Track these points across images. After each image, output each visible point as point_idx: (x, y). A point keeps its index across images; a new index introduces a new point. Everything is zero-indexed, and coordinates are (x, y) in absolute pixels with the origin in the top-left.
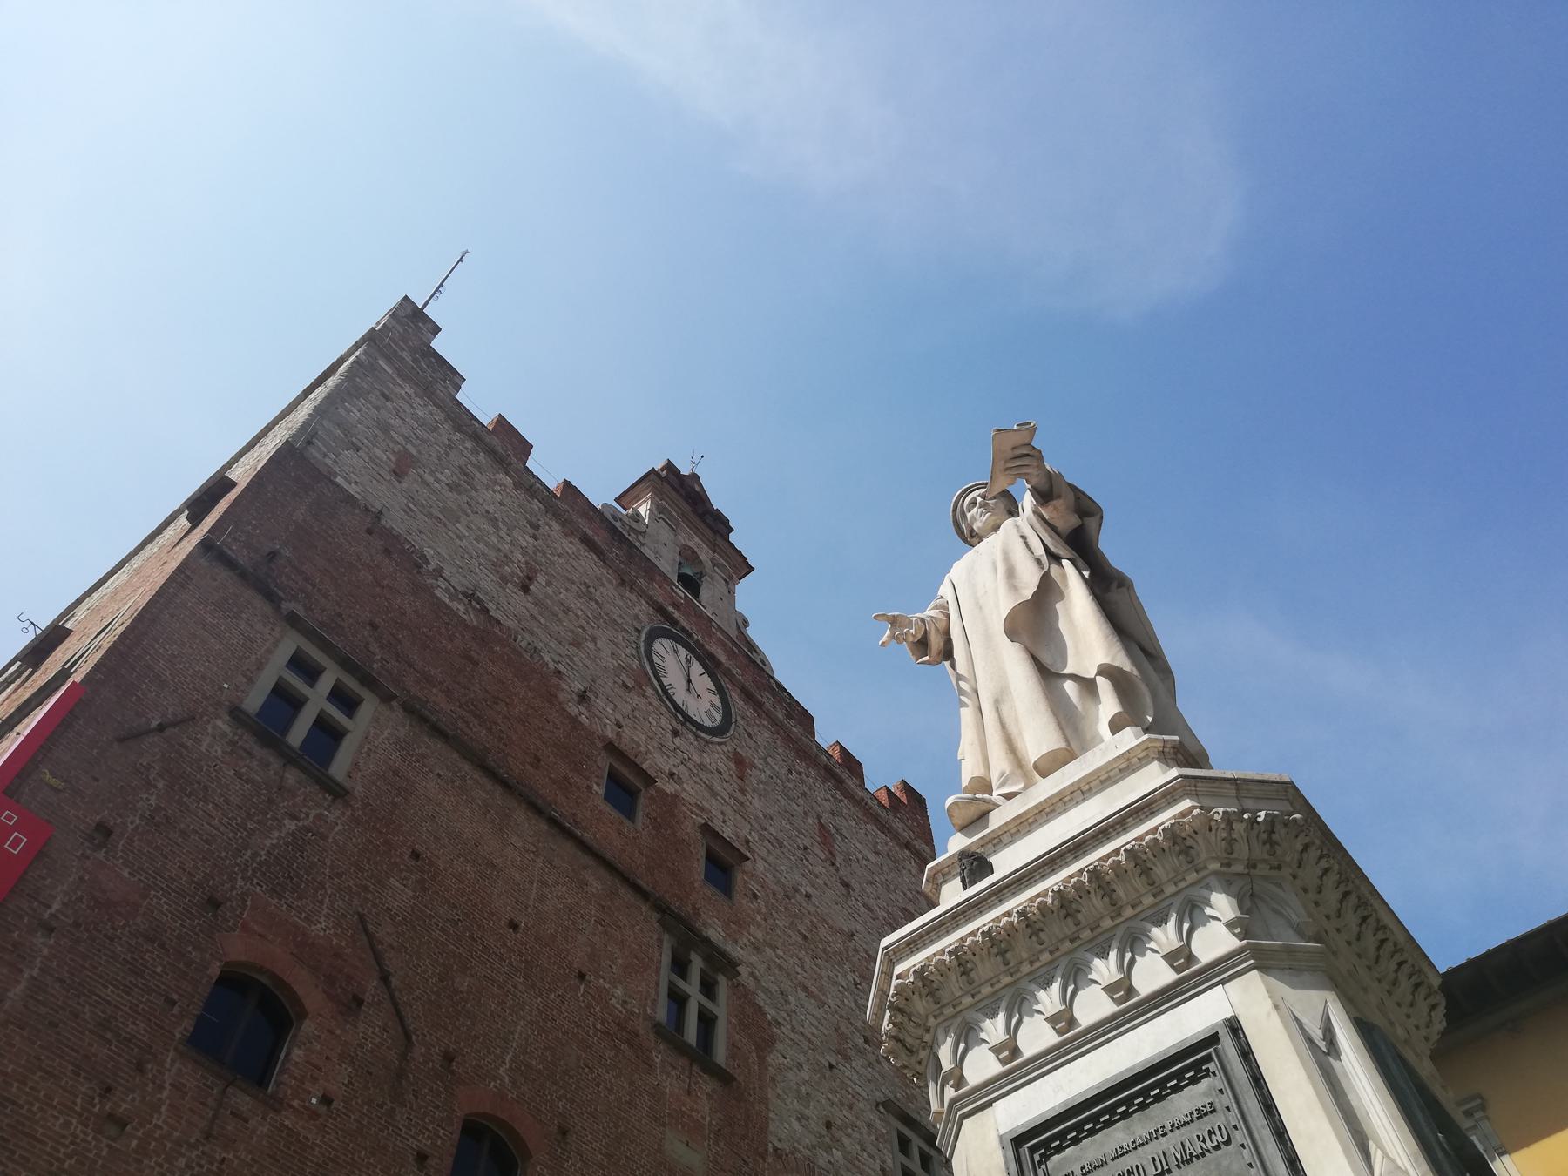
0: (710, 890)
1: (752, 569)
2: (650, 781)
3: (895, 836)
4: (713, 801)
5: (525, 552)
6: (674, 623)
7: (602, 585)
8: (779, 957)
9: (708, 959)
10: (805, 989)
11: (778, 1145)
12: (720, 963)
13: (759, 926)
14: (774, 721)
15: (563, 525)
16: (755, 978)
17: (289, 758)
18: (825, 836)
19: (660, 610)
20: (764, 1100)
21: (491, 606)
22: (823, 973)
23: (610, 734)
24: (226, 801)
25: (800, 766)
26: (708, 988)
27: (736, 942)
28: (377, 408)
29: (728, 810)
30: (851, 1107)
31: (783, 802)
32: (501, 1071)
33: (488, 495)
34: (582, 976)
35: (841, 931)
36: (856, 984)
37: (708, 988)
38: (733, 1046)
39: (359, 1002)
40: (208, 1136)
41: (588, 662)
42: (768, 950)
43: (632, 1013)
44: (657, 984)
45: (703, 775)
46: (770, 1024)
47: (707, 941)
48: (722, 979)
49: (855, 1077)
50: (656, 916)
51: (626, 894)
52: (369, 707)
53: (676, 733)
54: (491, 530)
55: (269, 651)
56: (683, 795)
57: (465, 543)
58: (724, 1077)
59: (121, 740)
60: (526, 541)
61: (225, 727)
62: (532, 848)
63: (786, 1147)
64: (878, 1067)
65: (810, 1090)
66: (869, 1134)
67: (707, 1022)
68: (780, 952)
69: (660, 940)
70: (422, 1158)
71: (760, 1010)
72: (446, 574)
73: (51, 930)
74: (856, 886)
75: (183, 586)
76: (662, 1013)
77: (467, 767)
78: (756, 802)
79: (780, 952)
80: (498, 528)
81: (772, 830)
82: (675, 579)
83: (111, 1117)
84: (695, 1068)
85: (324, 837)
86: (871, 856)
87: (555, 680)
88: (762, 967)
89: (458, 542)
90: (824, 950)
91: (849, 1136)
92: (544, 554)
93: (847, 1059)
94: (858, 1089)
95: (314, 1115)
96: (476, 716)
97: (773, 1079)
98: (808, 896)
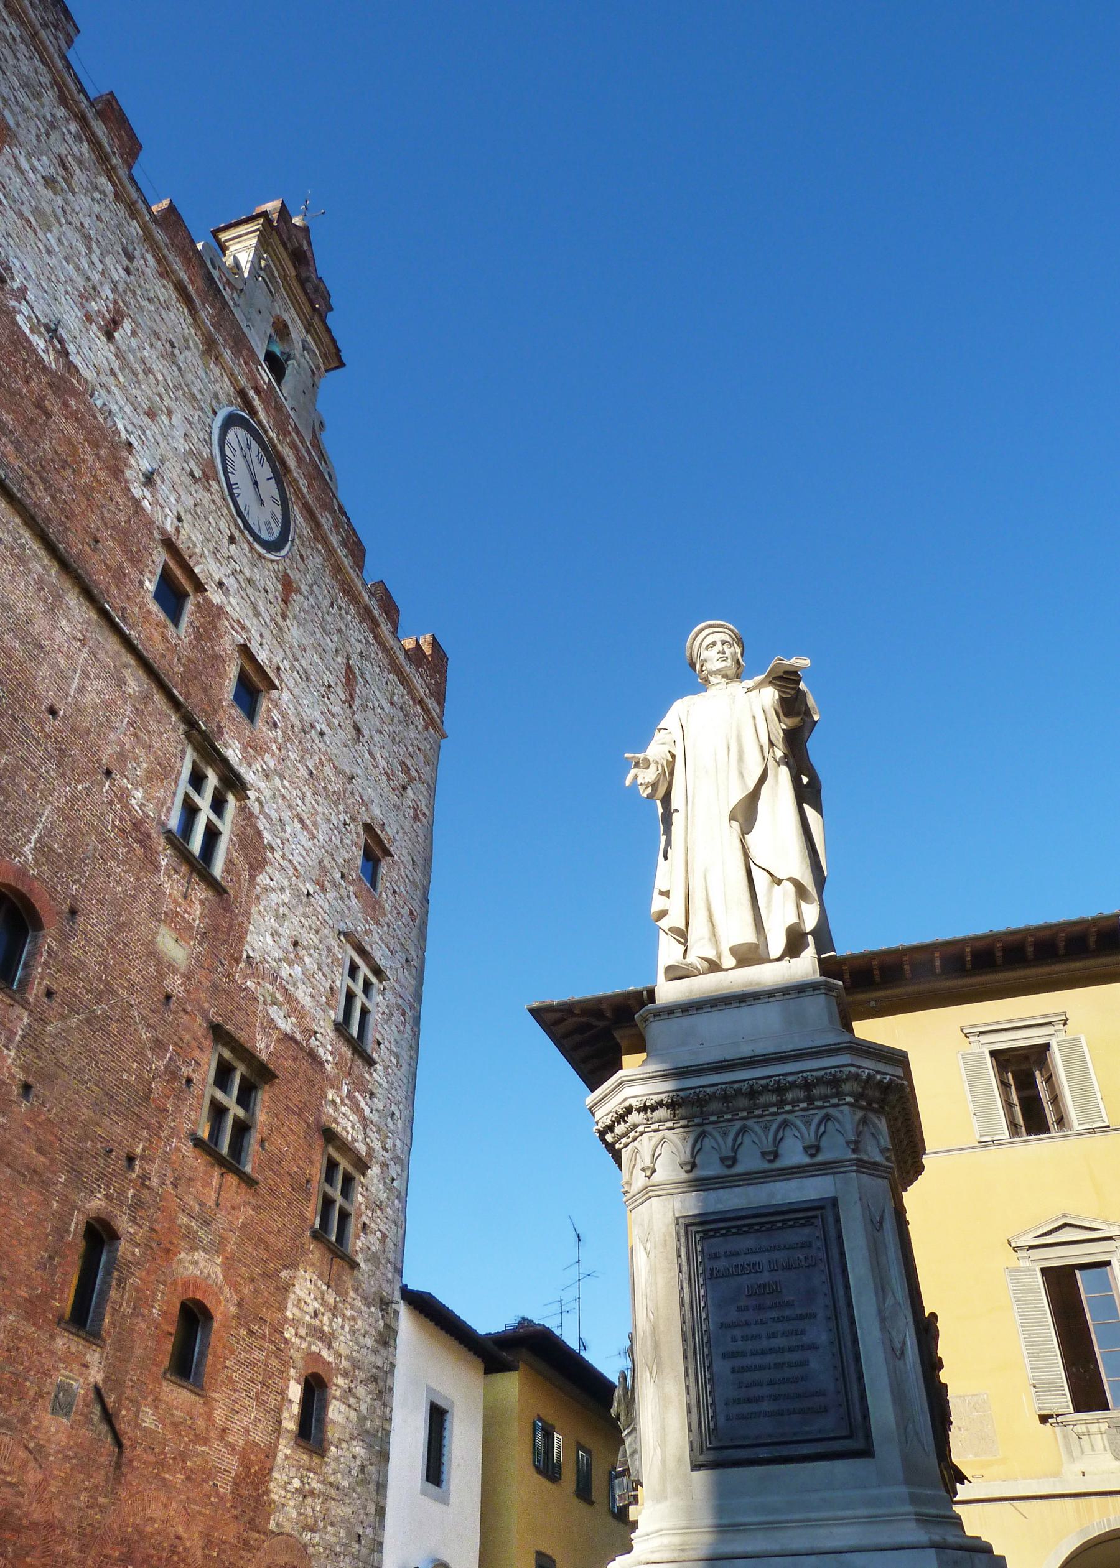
0: (236, 712)
3: (411, 691)
4: (255, 621)
8: (284, 787)
10: (301, 821)
11: (251, 954)
12: (233, 782)
13: (273, 755)
14: (330, 550)
16: (261, 803)
18: (350, 678)
19: (242, 393)
20: (248, 914)
22: (320, 809)
25: (343, 600)
26: (218, 805)
27: (250, 766)
29: (267, 634)
30: (317, 932)
31: (318, 635)
34: (108, 773)
36: (345, 824)
37: (218, 805)
38: (229, 862)
42: (277, 780)
43: (148, 816)
44: (174, 793)
46: (265, 847)
47: (225, 761)
48: (231, 798)
50: (182, 728)
57: (52, 261)
62: (79, 636)
63: (257, 956)
64: (347, 901)
66: (327, 957)
67: (212, 835)
68: (286, 783)
69: (184, 752)
71: (259, 834)
74: (366, 732)
76: (174, 822)
78: (294, 631)
79: (286, 783)
81: (303, 662)
82: (262, 357)
84: (195, 877)
88: (268, 794)
90: (325, 788)
91: (311, 955)
93: (323, 889)
94: (327, 917)
97: (258, 898)
98: (322, 734)
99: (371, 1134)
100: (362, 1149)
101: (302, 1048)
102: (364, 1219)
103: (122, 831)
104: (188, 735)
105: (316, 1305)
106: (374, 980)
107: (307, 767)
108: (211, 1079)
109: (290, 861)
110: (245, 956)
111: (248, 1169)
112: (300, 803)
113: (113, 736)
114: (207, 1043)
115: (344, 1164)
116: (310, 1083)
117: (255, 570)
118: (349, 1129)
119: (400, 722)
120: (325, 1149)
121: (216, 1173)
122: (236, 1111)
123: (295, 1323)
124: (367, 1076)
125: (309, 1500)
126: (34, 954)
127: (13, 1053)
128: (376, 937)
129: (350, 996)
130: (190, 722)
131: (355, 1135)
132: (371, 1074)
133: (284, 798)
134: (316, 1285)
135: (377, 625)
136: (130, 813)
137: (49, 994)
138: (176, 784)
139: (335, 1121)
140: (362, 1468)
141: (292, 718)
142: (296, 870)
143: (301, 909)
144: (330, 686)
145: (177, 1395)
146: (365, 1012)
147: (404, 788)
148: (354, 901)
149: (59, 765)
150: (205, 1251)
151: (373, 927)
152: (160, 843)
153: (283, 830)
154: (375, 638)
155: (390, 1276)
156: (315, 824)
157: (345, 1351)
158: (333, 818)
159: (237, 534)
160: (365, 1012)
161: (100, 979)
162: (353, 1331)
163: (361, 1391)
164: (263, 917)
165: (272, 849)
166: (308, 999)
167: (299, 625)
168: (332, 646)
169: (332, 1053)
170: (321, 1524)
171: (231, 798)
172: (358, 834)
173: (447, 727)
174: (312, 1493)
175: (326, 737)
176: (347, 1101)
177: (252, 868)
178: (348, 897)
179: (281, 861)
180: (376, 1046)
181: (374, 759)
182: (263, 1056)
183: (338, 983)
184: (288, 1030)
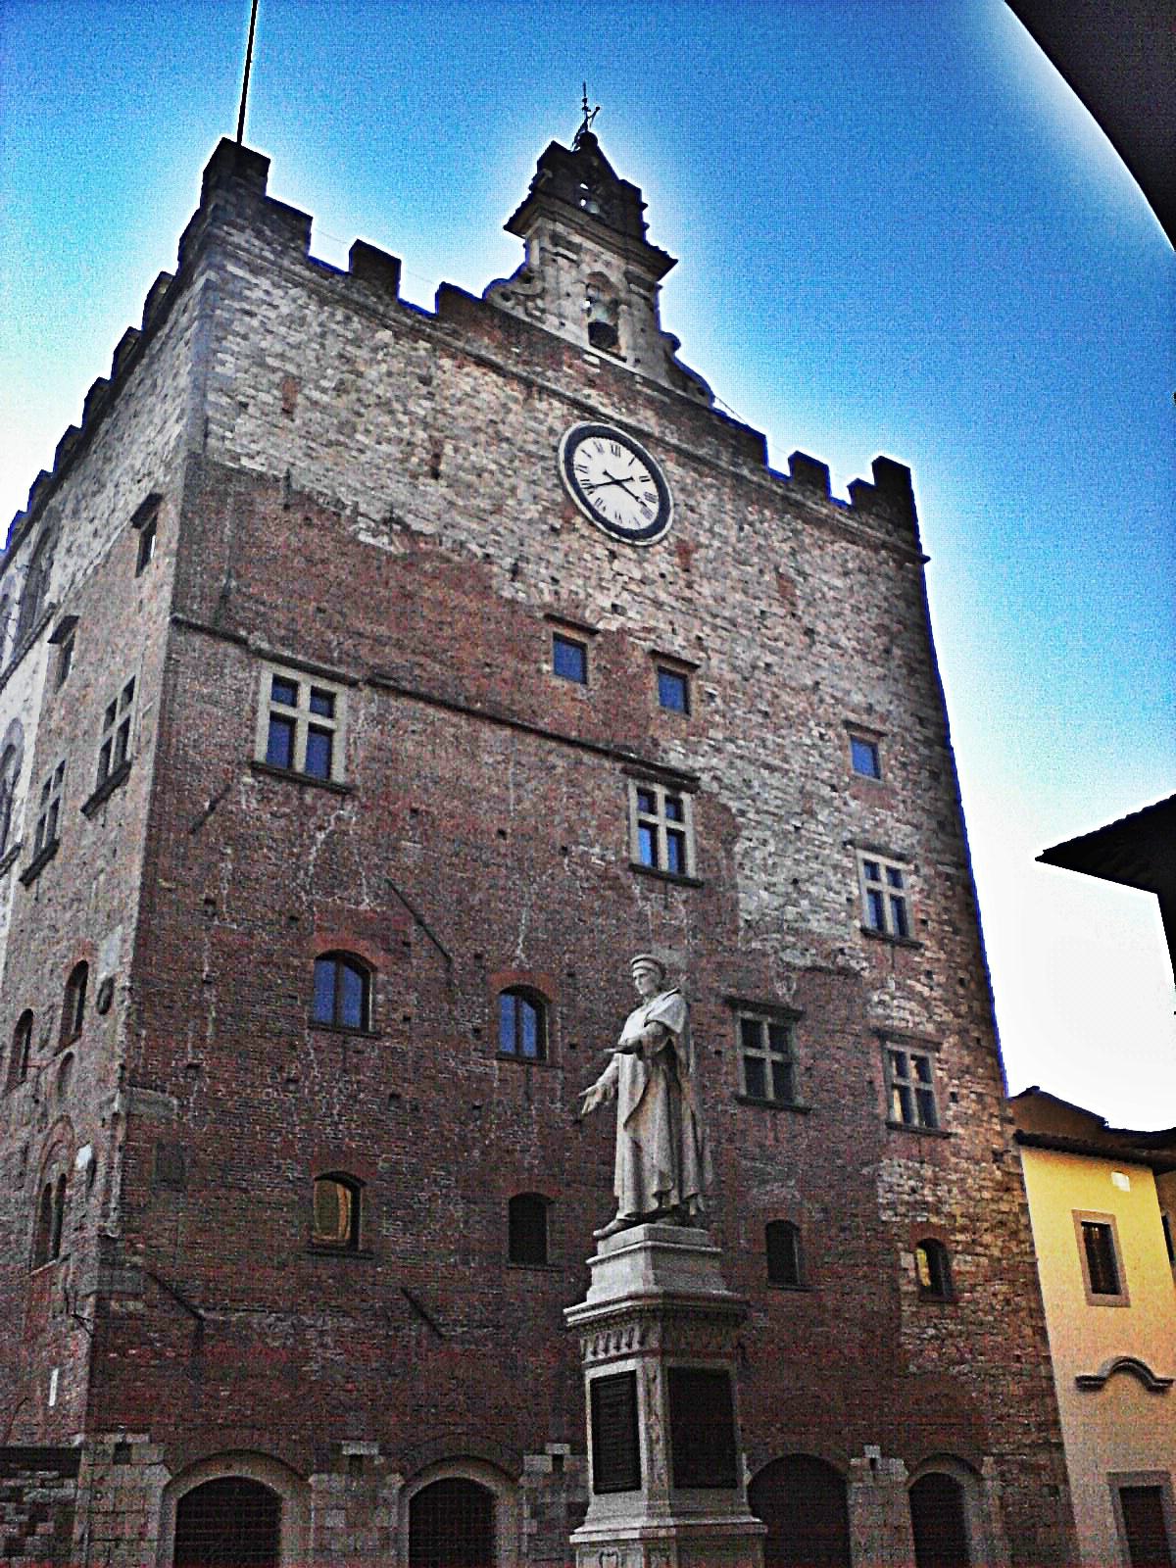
1: (674, 262)
2: (592, 632)
4: (660, 614)
5: (426, 426)
6: (592, 412)
7: (509, 411)
9: (668, 785)
15: (453, 357)
17: (302, 782)
20: (734, 887)
21: (409, 519)
22: (786, 742)
23: (548, 598)
24: (274, 840)
28: (245, 337)
29: (679, 619)
31: (735, 573)
32: (518, 952)
33: (372, 373)
34: (565, 851)
35: (804, 688)
38: (701, 851)
39: (407, 944)
40: (345, 1071)
41: (510, 524)
42: (731, 747)
43: (610, 863)
45: (647, 590)
48: (685, 797)
49: (821, 829)
50: (619, 766)
51: (588, 758)
52: (343, 699)
53: (613, 555)
54: (386, 419)
55: (256, 693)
56: (630, 624)
58: (694, 884)
59: (193, 832)
60: (422, 408)
61: (248, 780)
64: (844, 809)
65: (776, 859)
68: (741, 742)
69: (626, 787)
70: (477, 1031)
71: (726, 809)
72: (363, 508)
73: (209, 983)
74: (821, 628)
75: (176, 673)
77: (431, 710)
79: (741, 742)
80: (391, 412)
81: (727, 614)
83: (289, 1081)
84: (670, 886)
85: (345, 833)
86: (838, 583)
87: (487, 568)
88: (723, 765)
89: (363, 458)
92: (443, 412)
94: (825, 839)
95: (403, 1033)
96: (425, 654)
98: (768, 665)
99: (937, 1010)
100: (930, 1028)
101: (830, 972)
102: (951, 1090)
103: (594, 888)
104: (624, 771)
105: (912, 1183)
106: (900, 866)
107: (760, 711)
108: (739, 1042)
109: (767, 812)
110: (742, 924)
111: (800, 1101)
112: (761, 751)
113: (557, 819)
114: (728, 1013)
115: (908, 1051)
116: (850, 1001)
117: (645, 565)
118: (909, 1017)
119: (863, 586)
120: (882, 1047)
121: (768, 1115)
122: (770, 1056)
123: (891, 1206)
124: (917, 959)
125: (948, 1342)
126: (553, 1023)
127: (559, 1105)
128: (889, 820)
129: (876, 896)
130: (619, 758)
131: (917, 1019)
132: (923, 955)
133: (742, 757)
134: (907, 1168)
135: (799, 505)
136: (593, 869)
137: (573, 1046)
138: (628, 819)
139: (889, 1017)
140: (1008, 1302)
141: (729, 676)
142: (774, 814)
143: (791, 849)
144: (762, 612)
145: (784, 1298)
146: (898, 902)
147: (887, 651)
148: (853, 804)
149: (521, 871)
150: (776, 1180)
151: (884, 813)
152: (627, 878)
153: (750, 787)
154: (805, 521)
155: (998, 1128)
156: (786, 760)
157: (957, 1210)
158: (808, 742)
159: (610, 545)
160: (898, 902)
161: (611, 1015)
162: (963, 1191)
163: (987, 1238)
164: (751, 878)
165: (742, 813)
166: (824, 923)
167: (709, 579)
168: (756, 568)
169: (866, 959)
170: (968, 1356)
171: (685, 797)
172: (839, 736)
173: (926, 552)
174: (951, 1335)
175: (776, 669)
176: (898, 994)
177: (723, 842)
178: (845, 804)
179: (757, 818)
180: (920, 926)
181: (839, 647)
182: (788, 999)
183: (856, 892)
184: (809, 963)
